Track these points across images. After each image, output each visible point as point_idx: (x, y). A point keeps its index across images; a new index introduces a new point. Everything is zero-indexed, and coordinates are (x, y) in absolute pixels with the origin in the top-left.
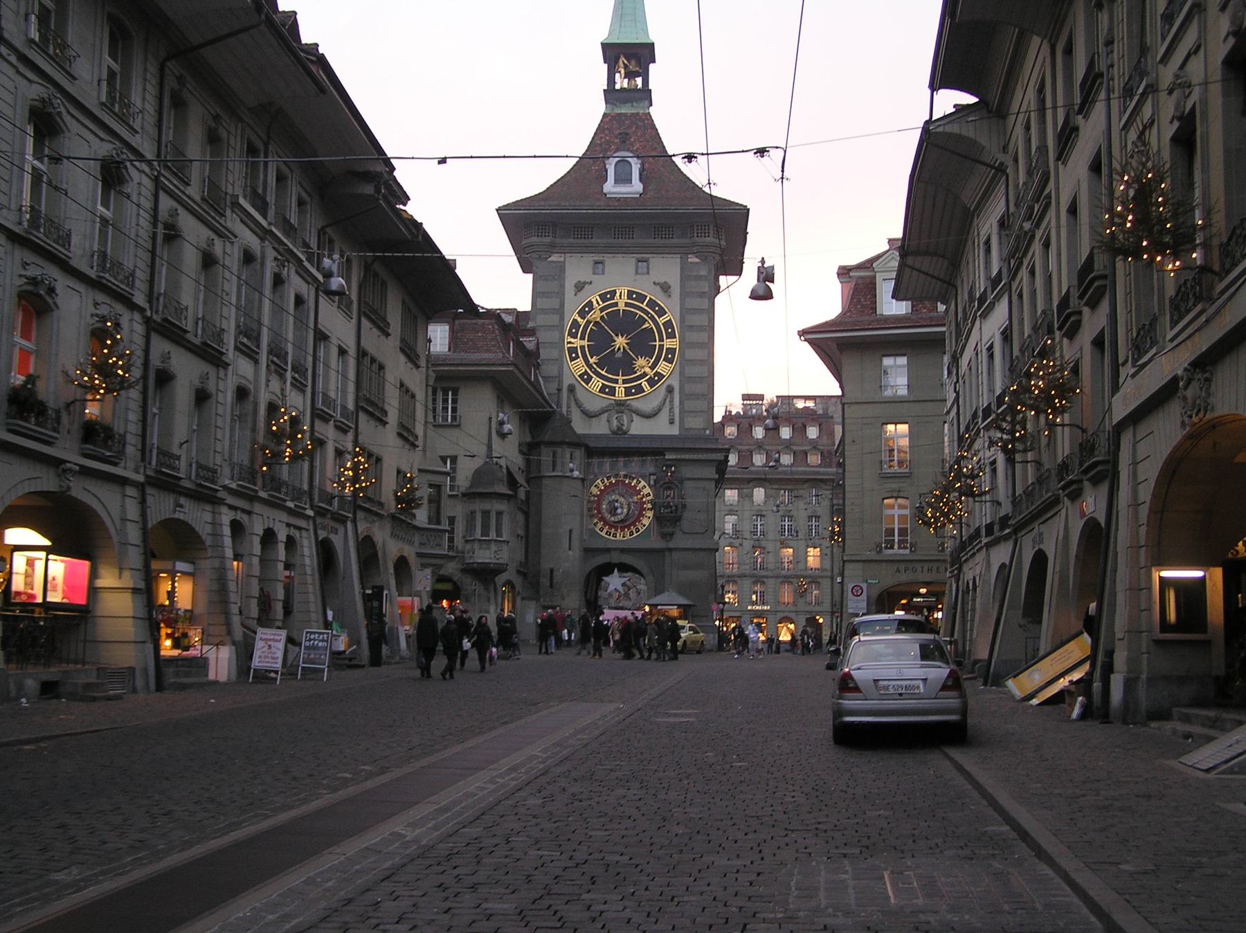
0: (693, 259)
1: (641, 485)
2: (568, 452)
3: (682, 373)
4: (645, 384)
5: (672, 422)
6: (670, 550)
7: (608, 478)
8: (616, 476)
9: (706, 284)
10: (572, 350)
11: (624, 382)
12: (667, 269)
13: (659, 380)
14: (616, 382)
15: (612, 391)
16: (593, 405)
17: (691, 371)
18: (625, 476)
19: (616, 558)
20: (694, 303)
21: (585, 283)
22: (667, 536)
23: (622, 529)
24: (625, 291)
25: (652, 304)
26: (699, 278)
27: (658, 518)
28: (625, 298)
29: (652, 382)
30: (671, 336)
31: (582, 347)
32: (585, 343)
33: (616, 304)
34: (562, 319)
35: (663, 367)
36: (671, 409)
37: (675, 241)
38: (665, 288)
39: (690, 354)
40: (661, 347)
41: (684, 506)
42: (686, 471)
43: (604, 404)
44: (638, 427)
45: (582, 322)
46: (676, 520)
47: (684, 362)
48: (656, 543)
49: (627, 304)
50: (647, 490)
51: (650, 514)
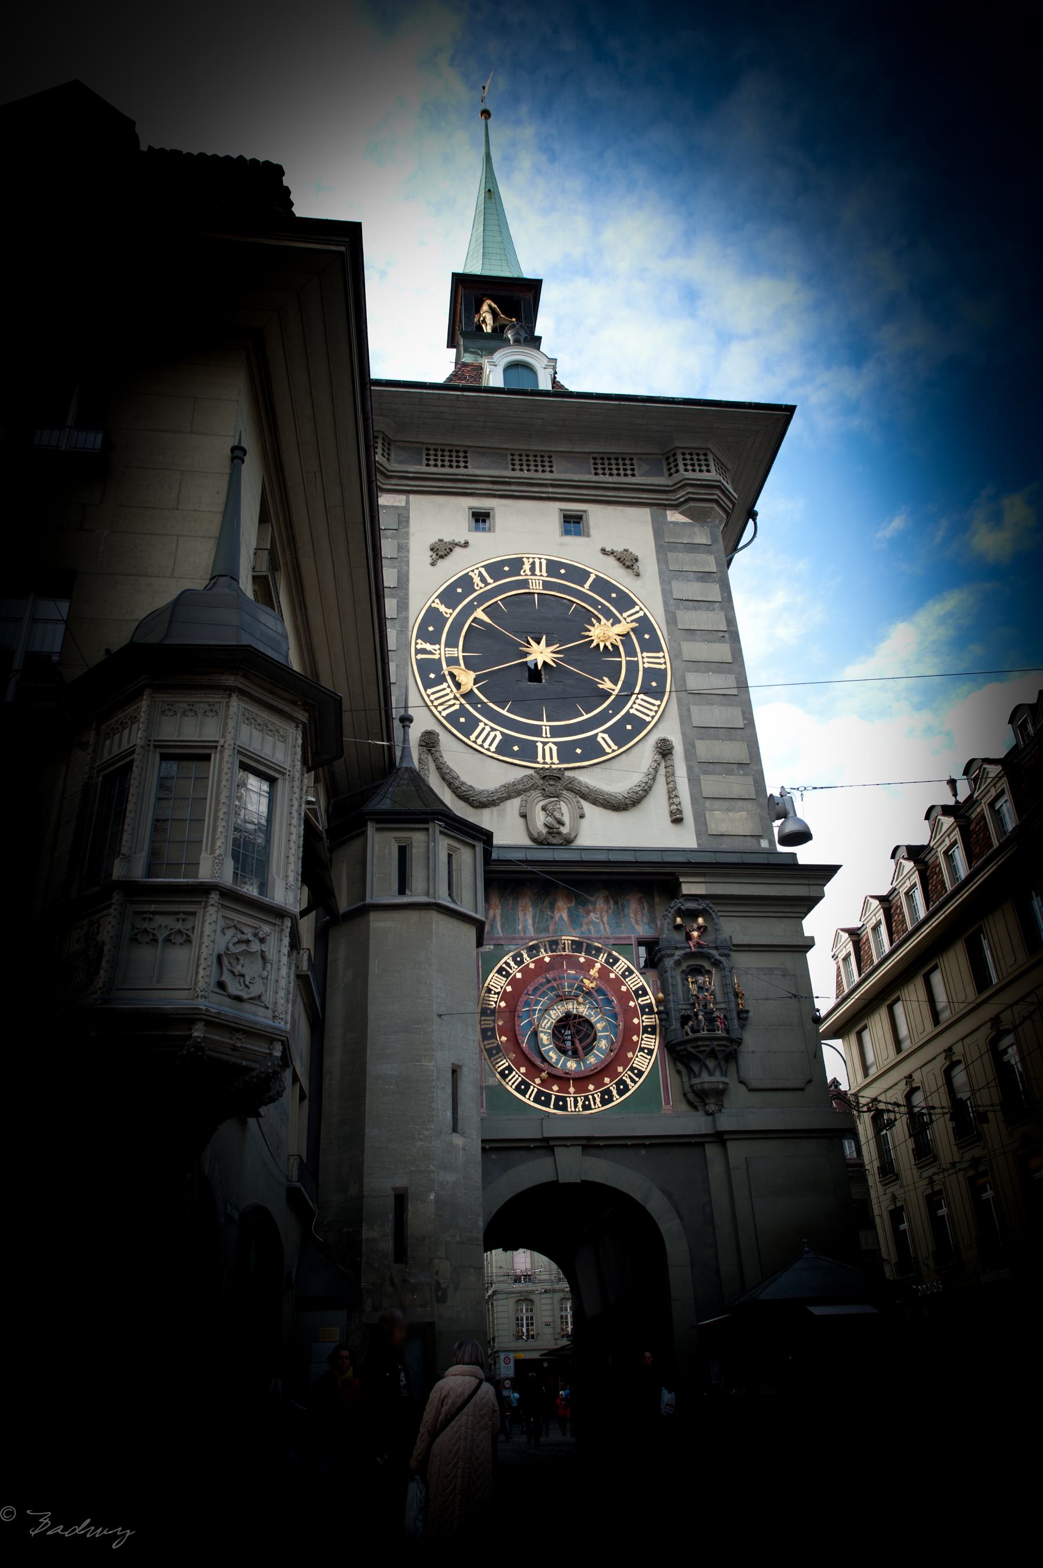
0: (674, 516)
2: (443, 845)
3: (685, 718)
4: (603, 739)
6: (720, 1138)
7: (533, 950)
8: (553, 945)
9: (711, 559)
11: (555, 732)
14: (537, 731)
15: (529, 752)
17: (705, 715)
18: (577, 946)
19: (572, 1167)
20: (693, 590)
22: (700, 1099)
23: (581, 1088)
25: (602, 586)
28: (542, 575)
29: (620, 736)
30: (652, 645)
32: (459, 653)
33: (525, 584)
36: (672, 794)
38: (628, 562)
39: (695, 681)
40: (633, 667)
41: (743, 1016)
42: (735, 928)
43: (514, 775)
44: (599, 832)
45: (450, 614)
46: (728, 1053)
48: (676, 1119)
49: (546, 585)
50: (636, 980)
51: (652, 1042)
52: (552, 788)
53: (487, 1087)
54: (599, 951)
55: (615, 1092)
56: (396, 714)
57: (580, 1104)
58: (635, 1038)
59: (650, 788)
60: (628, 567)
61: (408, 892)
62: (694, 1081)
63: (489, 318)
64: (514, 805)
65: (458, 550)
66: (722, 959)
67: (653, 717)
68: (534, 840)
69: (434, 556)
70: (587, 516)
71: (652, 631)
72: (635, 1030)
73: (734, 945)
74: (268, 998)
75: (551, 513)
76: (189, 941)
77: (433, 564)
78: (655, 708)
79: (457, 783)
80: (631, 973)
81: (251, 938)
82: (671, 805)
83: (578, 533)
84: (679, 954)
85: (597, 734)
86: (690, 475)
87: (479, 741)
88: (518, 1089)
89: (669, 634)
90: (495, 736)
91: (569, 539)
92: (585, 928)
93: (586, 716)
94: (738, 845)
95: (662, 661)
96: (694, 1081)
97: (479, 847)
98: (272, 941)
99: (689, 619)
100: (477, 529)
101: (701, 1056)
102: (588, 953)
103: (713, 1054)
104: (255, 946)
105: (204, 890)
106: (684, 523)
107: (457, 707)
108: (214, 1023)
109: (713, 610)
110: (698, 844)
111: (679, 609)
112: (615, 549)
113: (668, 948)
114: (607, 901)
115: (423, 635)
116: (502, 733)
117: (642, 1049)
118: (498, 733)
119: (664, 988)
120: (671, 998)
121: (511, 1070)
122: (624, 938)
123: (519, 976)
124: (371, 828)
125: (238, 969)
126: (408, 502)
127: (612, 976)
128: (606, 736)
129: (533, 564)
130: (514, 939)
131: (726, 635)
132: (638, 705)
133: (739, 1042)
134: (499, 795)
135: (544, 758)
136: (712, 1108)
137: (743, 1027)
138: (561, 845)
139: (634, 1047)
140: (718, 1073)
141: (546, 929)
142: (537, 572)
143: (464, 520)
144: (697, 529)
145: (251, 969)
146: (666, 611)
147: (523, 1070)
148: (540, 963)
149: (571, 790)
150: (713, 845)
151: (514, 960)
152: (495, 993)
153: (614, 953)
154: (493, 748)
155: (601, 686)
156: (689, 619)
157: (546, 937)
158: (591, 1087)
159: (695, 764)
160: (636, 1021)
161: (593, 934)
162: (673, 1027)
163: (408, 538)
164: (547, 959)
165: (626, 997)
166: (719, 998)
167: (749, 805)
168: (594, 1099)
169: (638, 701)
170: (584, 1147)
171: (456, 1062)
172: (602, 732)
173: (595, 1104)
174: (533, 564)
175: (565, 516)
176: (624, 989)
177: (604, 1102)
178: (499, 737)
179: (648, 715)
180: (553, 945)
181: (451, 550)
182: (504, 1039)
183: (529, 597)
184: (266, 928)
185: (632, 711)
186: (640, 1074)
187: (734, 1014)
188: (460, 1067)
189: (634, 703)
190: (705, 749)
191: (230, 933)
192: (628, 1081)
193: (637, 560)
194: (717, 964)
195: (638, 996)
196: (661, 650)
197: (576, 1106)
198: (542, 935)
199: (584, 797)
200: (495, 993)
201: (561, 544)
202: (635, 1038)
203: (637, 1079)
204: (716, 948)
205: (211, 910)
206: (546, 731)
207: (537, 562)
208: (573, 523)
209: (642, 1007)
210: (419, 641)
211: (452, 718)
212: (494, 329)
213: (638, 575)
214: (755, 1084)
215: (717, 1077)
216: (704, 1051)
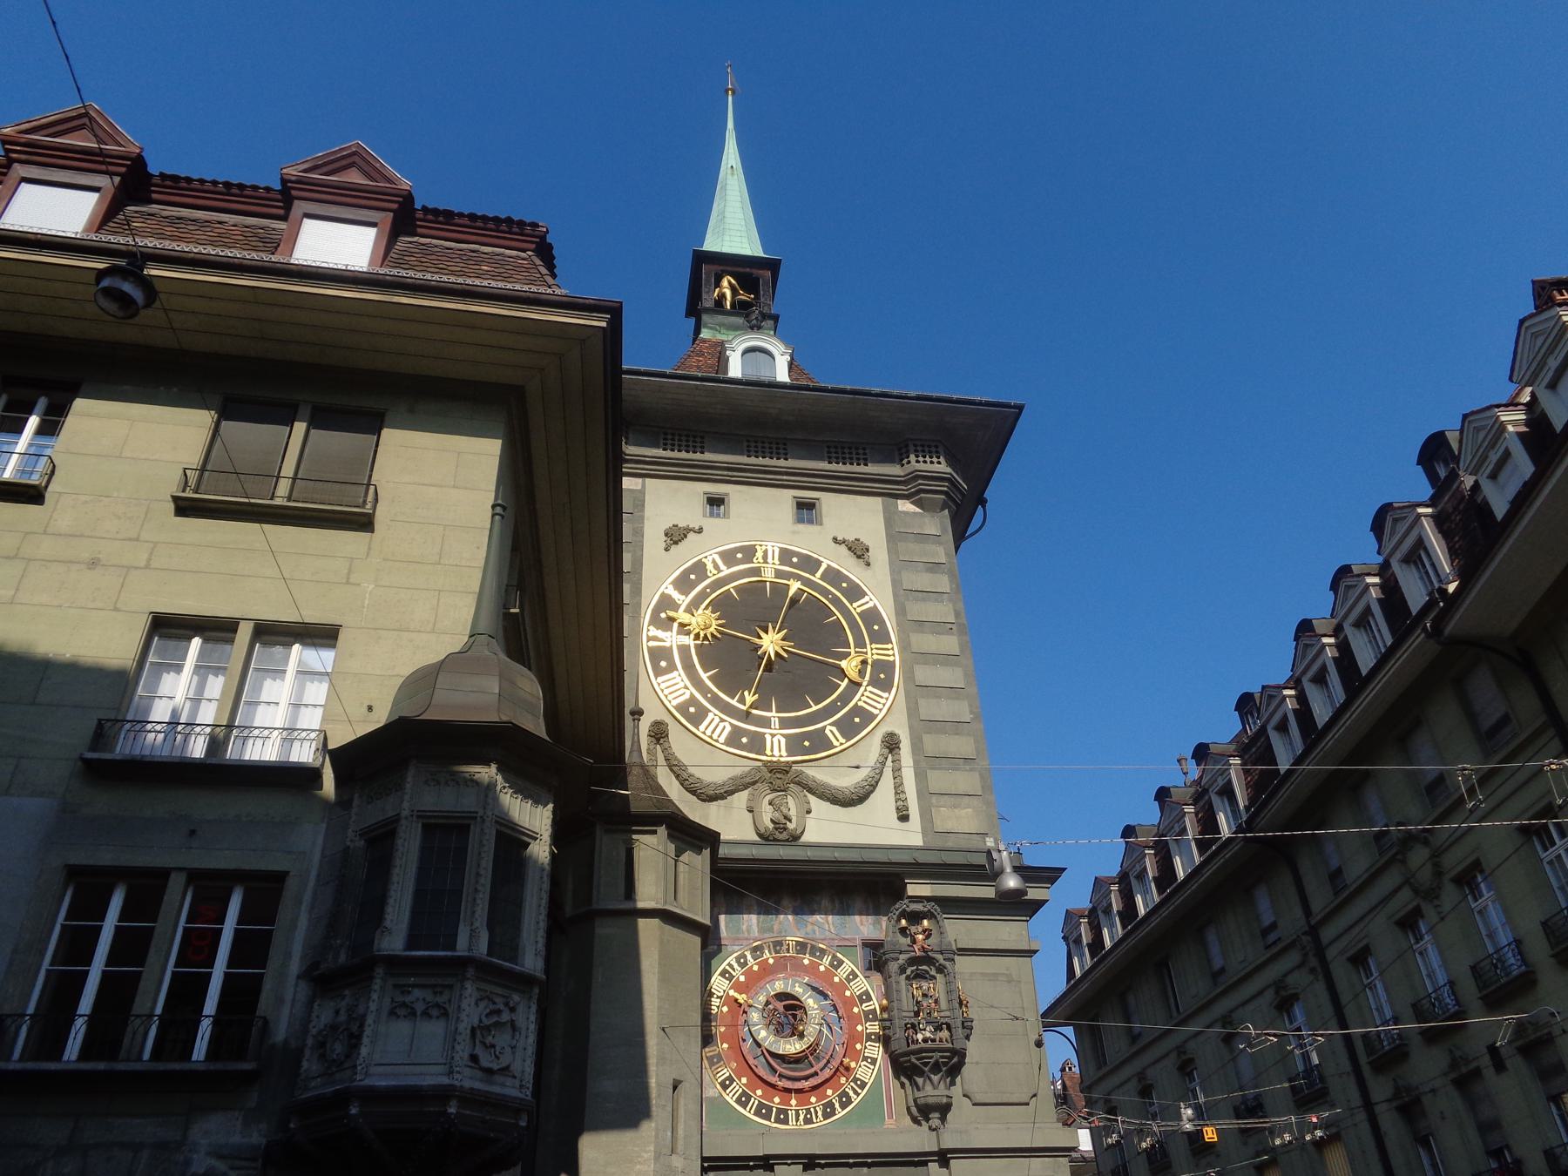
0: (905, 506)
1: (842, 973)
3: (912, 710)
4: (831, 732)
5: (904, 818)
6: (943, 1157)
8: (778, 945)
10: (659, 654)
11: (785, 723)
12: (855, 516)
14: (765, 723)
15: (757, 744)
16: (714, 774)
18: (801, 947)
21: (689, 530)
22: (924, 1112)
24: (773, 549)
25: (833, 576)
26: (923, 537)
27: (905, 1066)
30: (881, 637)
31: (684, 650)
33: (756, 572)
36: (899, 789)
37: (872, 469)
38: (859, 551)
39: (924, 674)
42: (959, 930)
44: (825, 829)
46: (952, 1064)
47: (917, 691)
49: (779, 574)
50: (861, 984)
51: (876, 1051)
56: (629, 706)
58: (858, 1046)
62: (918, 1094)
63: (728, 293)
64: (742, 798)
65: (691, 536)
66: (947, 964)
68: (760, 835)
71: (882, 623)
74: (516, 1067)
75: (784, 500)
76: (445, 1014)
77: (666, 550)
79: (685, 776)
81: (502, 1007)
83: (810, 522)
84: (903, 957)
86: (921, 466)
87: (709, 732)
88: (738, 1101)
91: (801, 527)
92: (810, 927)
93: (815, 708)
94: (963, 843)
96: (918, 1094)
97: (707, 852)
98: (521, 1009)
99: (918, 610)
100: (712, 515)
103: (936, 1068)
104: (505, 1017)
105: (462, 963)
107: (687, 696)
108: (470, 1099)
113: (893, 951)
114: (833, 901)
115: (656, 621)
117: (865, 1059)
119: (887, 995)
120: (895, 1004)
121: (732, 1081)
123: (742, 978)
124: (599, 831)
125: (489, 1039)
126: (644, 485)
132: (866, 697)
133: (962, 1054)
139: (856, 1055)
140: (942, 1085)
141: (771, 930)
142: (770, 560)
143: (699, 504)
145: (502, 1039)
147: (744, 1080)
149: (799, 784)
150: (939, 844)
154: (722, 739)
156: (918, 610)
157: (770, 937)
158: (813, 1099)
161: (818, 935)
164: (771, 961)
165: (850, 1002)
166: (943, 1004)
167: (975, 801)
170: (806, 1168)
174: (766, 552)
176: (848, 993)
177: (826, 1116)
178: (728, 729)
180: (778, 945)
182: (725, 1046)
184: (516, 997)
190: (932, 744)
191: (482, 1005)
194: (941, 969)
201: (794, 532)
204: (941, 952)
205: (468, 985)
208: (806, 510)
209: (866, 1014)
211: (683, 708)
212: (733, 305)
213: (868, 564)
214: (979, 1099)
215: (942, 1090)
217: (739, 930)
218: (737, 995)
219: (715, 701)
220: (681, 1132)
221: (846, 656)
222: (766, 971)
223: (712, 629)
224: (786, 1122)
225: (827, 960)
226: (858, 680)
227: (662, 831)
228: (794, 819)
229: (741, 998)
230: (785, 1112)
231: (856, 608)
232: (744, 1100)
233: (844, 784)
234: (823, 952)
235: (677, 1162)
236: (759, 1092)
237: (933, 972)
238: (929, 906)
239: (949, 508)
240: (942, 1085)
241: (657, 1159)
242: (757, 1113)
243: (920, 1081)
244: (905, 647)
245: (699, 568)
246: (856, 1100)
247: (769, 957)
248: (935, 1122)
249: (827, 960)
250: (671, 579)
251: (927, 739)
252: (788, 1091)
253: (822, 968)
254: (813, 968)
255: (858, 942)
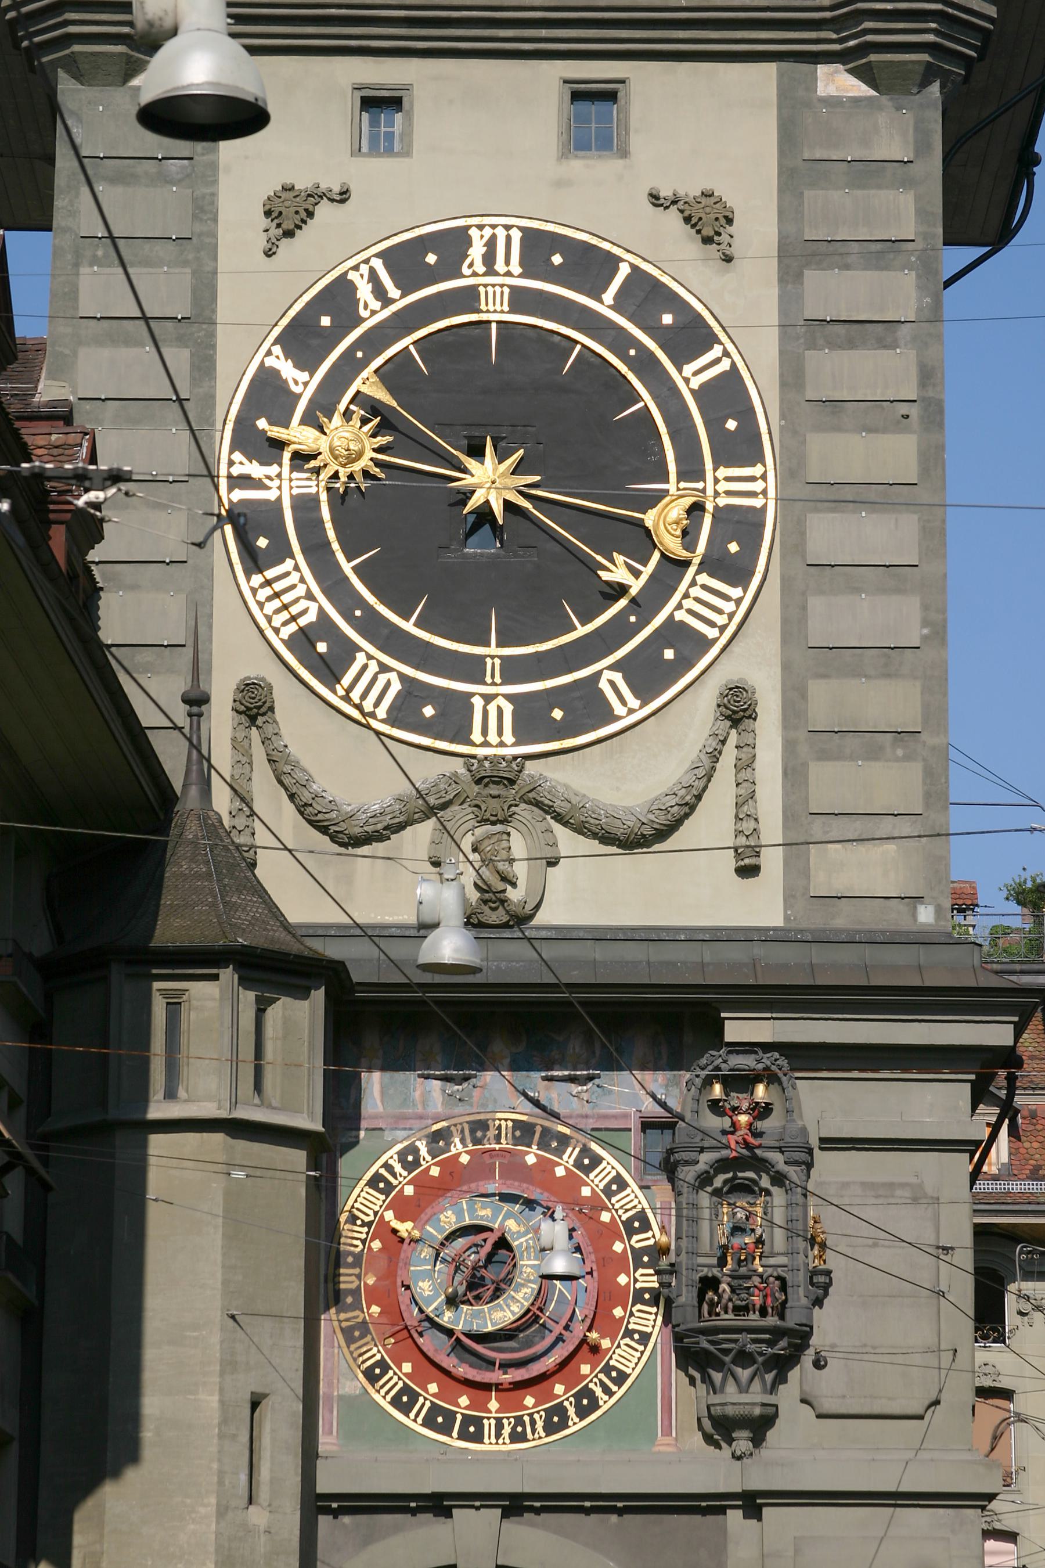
0: (836, 82)
4: (610, 679)
6: (752, 1503)
9: (905, 202)
11: (513, 670)
13: (684, 663)
14: (472, 669)
15: (454, 719)
18: (524, 1132)
21: (317, 195)
25: (645, 295)
26: (867, 172)
28: (511, 271)
29: (647, 675)
30: (740, 448)
31: (305, 505)
33: (468, 298)
34: (205, 365)
35: (698, 601)
38: (708, 222)
49: (520, 299)
50: (633, 1198)
51: (649, 1320)
52: (494, 804)
53: (341, 1398)
54: (564, 1141)
55: (571, 1411)
57: (507, 1431)
58: (618, 1312)
59: (699, 798)
60: (707, 240)
61: (182, 1093)
65: (324, 210)
67: (723, 629)
69: (275, 232)
70: (627, 95)
72: (619, 1296)
73: (822, 1140)
78: (729, 607)
79: (306, 796)
80: (623, 1185)
82: (738, 833)
84: (706, 1159)
85: (599, 673)
88: (396, 1402)
89: (783, 416)
90: (388, 684)
91: (577, 166)
93: (581, 631)
95: (758, 486)
100: (374, 150)
101: (727, 1359)
102: (543, 1145)
106: (856, 101)
107: (311, 617)
109: (894, 346)
110: (787, 918)
111: (812, 345)
112: (681, 193)
113: (687, 1149)
116: (402, 677)
117: (629, 1333)
118: (393, 676)
120: (684, 1243)
121: (384, 1367)
122: (615, 1117)
123: (409, 1190)
127: (586, 1192)
128: (618, 677)
129: (491, 243)
130: (405, 1118)
131: (914, 411)
132: (696, 599)
134: (387, 820)
135: (485, 732)
136: (742, 1444)
137: (818, 1302)
138: (506, 926)
142: (500, 266)
144: (882, 119)
146: (781, 352)
147: (407, 1367)
148: (450, 1165)
151: (402, 1156)
152: (364, 1224)
153: (594, 1146)
155: (604, 575)
158: (529, 1401)
159: (802, 735)
160: (622, 1280)
162: (682, 1300)
163: (215, 182)
164: (465, 1159)
168: (533, 1423)
169: (696, 592)
171: (259, 1389)
172: (610, 668)
173: (534, 1431)
174: (491, 243)
175: (577, 96)
177: (550, 1428)
178: (396, 686)
179: (712, 624)
180: (479, 1128)
181: (310, 214)
182: (375, 1309)
183: (477, 331)
185: (679, 616)
186: (621, 1378)
187: (801, 1277)
188: (265, 1396)
189: (686, 596)
190: (825, 701)
192: (598, 1391)
193: (730, 221)
194: (779, 1179)
195: (631, 1232)
196: (757, 457)
197: (498, 1435)
198: (460, 1109)
199: (559, 818)
200: (364, 1224)
201: (560, 184)
202: (618, 1312)
203: (614, 1388)
206: (493, 667)
207: (501, 233)
209: (637, 1254)
210: (237, 456)
213: (728, 259)
214: (829, 1405)
216: (729, 1351)
217: (406, 1100)
218: (395, 1224)
219: (373, 628)
220: (265, 1472)
221: (653, 500)
222: (453, 1179)
223: (364, 462)
224: (478, 1438)
225: (570, 1156)
226: (684, 554)
227: (228, 974)
228: (522, 882)
229: (404, 1228)
230: (478, 1422)
231: (690, 377)
232: (405, 1400)
233: (628, 802)
234: (564, 1141)
235: (257, 1516)
236: (433, 1388)
237: (765, 1182)
238: (768, 1059)
239: (945, 77)
240: (756, 1385)
241: (222, 1512)
242: (429, 1422)
243: (717, 1377)
244: (791, 470)
245: (339, 297)
246: (606, 1403)
247: (460, 1150)
248: (742, 1444)
249: (570, 1156)
250: (277, 331)
251: (820, 692)
252: (486, 1387)
253: (560, 1172)
254: (545, 1167)
255: (634, 1124)
